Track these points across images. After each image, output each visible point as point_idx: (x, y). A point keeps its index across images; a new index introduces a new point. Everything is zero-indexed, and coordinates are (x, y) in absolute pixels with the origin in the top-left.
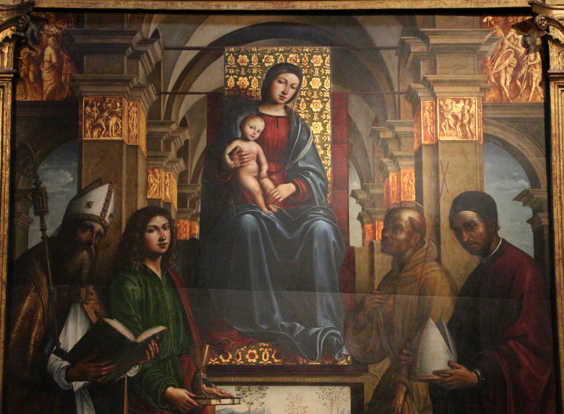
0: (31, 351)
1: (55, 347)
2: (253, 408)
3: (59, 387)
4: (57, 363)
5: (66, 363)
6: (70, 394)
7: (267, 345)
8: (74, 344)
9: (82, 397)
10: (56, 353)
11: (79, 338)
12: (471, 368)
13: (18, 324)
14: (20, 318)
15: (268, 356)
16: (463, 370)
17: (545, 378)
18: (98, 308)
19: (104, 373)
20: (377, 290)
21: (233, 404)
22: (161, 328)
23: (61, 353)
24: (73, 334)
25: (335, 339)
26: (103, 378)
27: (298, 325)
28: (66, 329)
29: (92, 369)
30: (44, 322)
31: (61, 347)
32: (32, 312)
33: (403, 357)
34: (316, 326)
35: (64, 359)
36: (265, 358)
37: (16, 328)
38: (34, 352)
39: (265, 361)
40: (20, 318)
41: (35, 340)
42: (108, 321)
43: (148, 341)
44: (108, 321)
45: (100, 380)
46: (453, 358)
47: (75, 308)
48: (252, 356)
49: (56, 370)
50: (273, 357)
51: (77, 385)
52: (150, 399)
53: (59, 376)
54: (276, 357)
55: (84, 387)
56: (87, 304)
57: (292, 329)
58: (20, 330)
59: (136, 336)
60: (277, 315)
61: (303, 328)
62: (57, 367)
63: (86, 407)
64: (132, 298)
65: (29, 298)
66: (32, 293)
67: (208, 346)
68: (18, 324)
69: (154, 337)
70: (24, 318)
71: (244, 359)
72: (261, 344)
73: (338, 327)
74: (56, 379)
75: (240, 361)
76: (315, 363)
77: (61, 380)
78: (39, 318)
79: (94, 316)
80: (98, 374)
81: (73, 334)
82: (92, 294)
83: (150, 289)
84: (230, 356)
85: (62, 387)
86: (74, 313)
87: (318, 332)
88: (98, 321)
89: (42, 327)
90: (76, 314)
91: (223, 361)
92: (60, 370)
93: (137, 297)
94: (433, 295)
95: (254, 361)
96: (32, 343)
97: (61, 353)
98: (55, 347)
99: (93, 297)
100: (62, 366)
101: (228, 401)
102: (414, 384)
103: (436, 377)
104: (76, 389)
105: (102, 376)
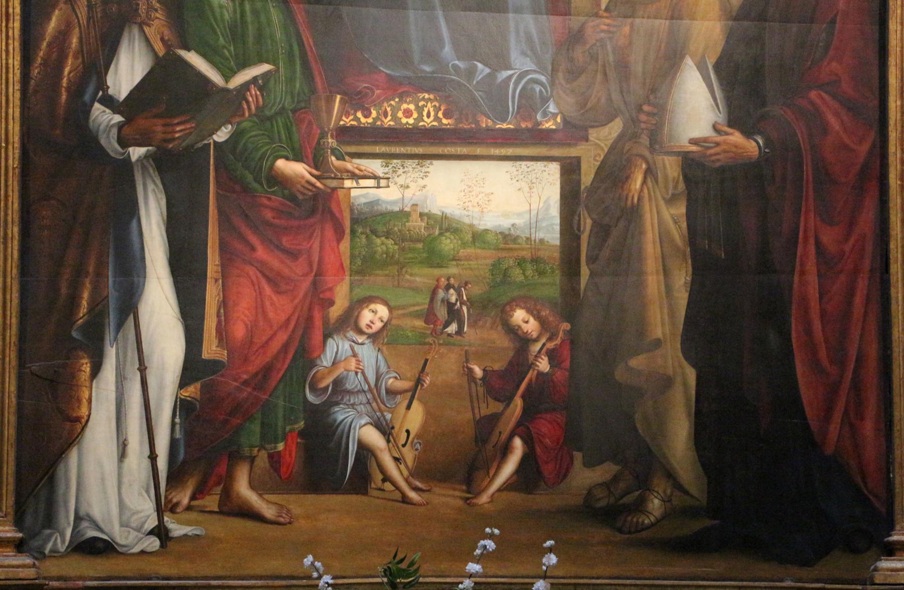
0: (64, 97)
1: (101, 93)
2: (408, 193)
3: (108, 155)
4: (103, 118)
5: (118, 118)
6: (126, 163)
7: (432, 96)
8: (131, 88)
9: (144, 169)
10: (101, 102)
11: (138, 79)
12: (748, 133)
13: (41, 54)
14: (45, 44)
15: (432, 114)
16: (736, 137)
17: (864, 149)
18: (167, 34)
19: (177, 135)
20: (607, 9)
21: (379, 187)
22: (265, 67)
23: (109, 102)
24: (127, 72)
25: (538, 88)
26: (176, 143)
27: (480, 65)
28: (117, 64)
29: (159, 128)
30: (82, 51)
31: (110, 92)
32: (63, 35)
33: (643, 117)
34: (508, 67)
35: (115, 111)
36: (428, 116)
37: (39, 60)
38: (67, 96)
39: (428, 122)
40: (45, 44)
41: (69, 80)
42: (183, 53)
43: (246, 86)
44: (183, 53)
45: (171, 146)
46: (721, 118)
47: (130, 32)
48: (408, 113)
49: (102, 127)
50: (440, 115)
51: (136, 153)
52: (250, 178)
53: (108, 137)
54: (446, 115)
55: (147, 156)
56: (149, 26)
57: (471, 73)
58: (45, 63)
59: (227, 79)
60: (447, 50)
61: (487, 70)
62: (105, 123)
63: (151, 186)
64: (219, 17)
65: (57, 12)
66: (62, 5)
67: (339, 97)
68: (41, 54)
69: (254, 80)
70: (49, 45)
71: (395, 118)
72: (421, 95)
73: (542, 70)
74: (103, 142)
75: (388, 122)
76: (505, 126)
77: (110, 144)
78: (74, 46)
79: (160, 44)
80: (169, 136)
81: (127, 72)
82: (156, 10)
83: (247, 7)
84: (374, 114)
85: (112, 154)
86: (129, 41)
87: (510, 77)
88: (167, 54)
89: (80, 60)
90: (131, 41)
91: (363, 120)
92: (109, 127)
93: (227, 17)
94: (693, 19)
95: (411, 121)
96: (64, 85)
97: (109, 102)
98: (101, 93)
99: (158, 15)
100: (113, 122)
101: (371, 182)
102: (659, 158)
103: (694, 148)
104: (134, 158)
105: (174, 139)
